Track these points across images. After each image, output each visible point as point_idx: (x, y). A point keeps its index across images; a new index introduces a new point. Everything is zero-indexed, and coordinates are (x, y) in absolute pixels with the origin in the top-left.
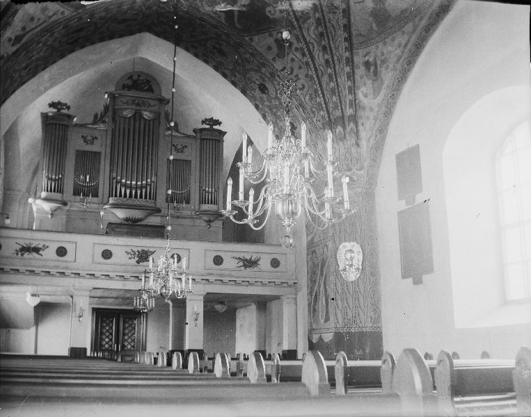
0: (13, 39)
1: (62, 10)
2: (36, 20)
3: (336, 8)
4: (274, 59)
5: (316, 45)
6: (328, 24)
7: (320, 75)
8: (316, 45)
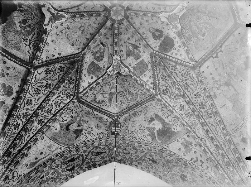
0: (29, 164)
1: (60, 147)
2: (44, 153)
3: (210, 114)
4: (184, 155)
5: (206, 139)
6: (209, 125)
7: (216, 157)
8: (206, 139)
